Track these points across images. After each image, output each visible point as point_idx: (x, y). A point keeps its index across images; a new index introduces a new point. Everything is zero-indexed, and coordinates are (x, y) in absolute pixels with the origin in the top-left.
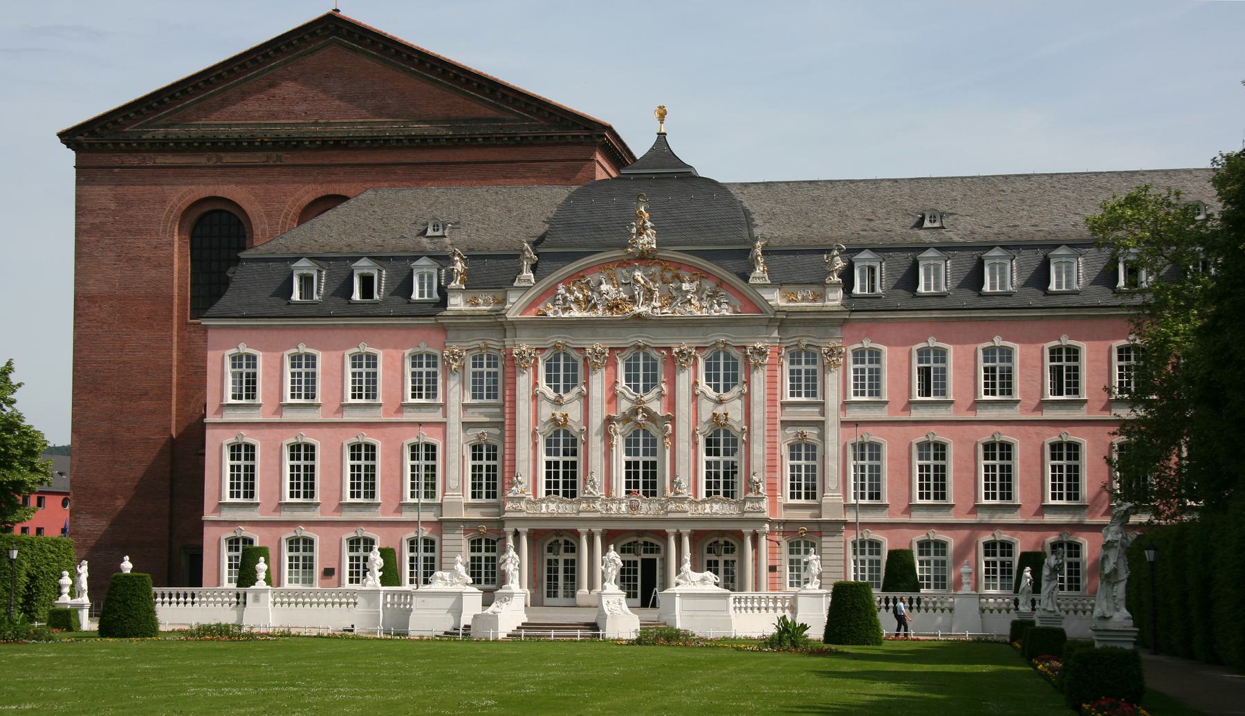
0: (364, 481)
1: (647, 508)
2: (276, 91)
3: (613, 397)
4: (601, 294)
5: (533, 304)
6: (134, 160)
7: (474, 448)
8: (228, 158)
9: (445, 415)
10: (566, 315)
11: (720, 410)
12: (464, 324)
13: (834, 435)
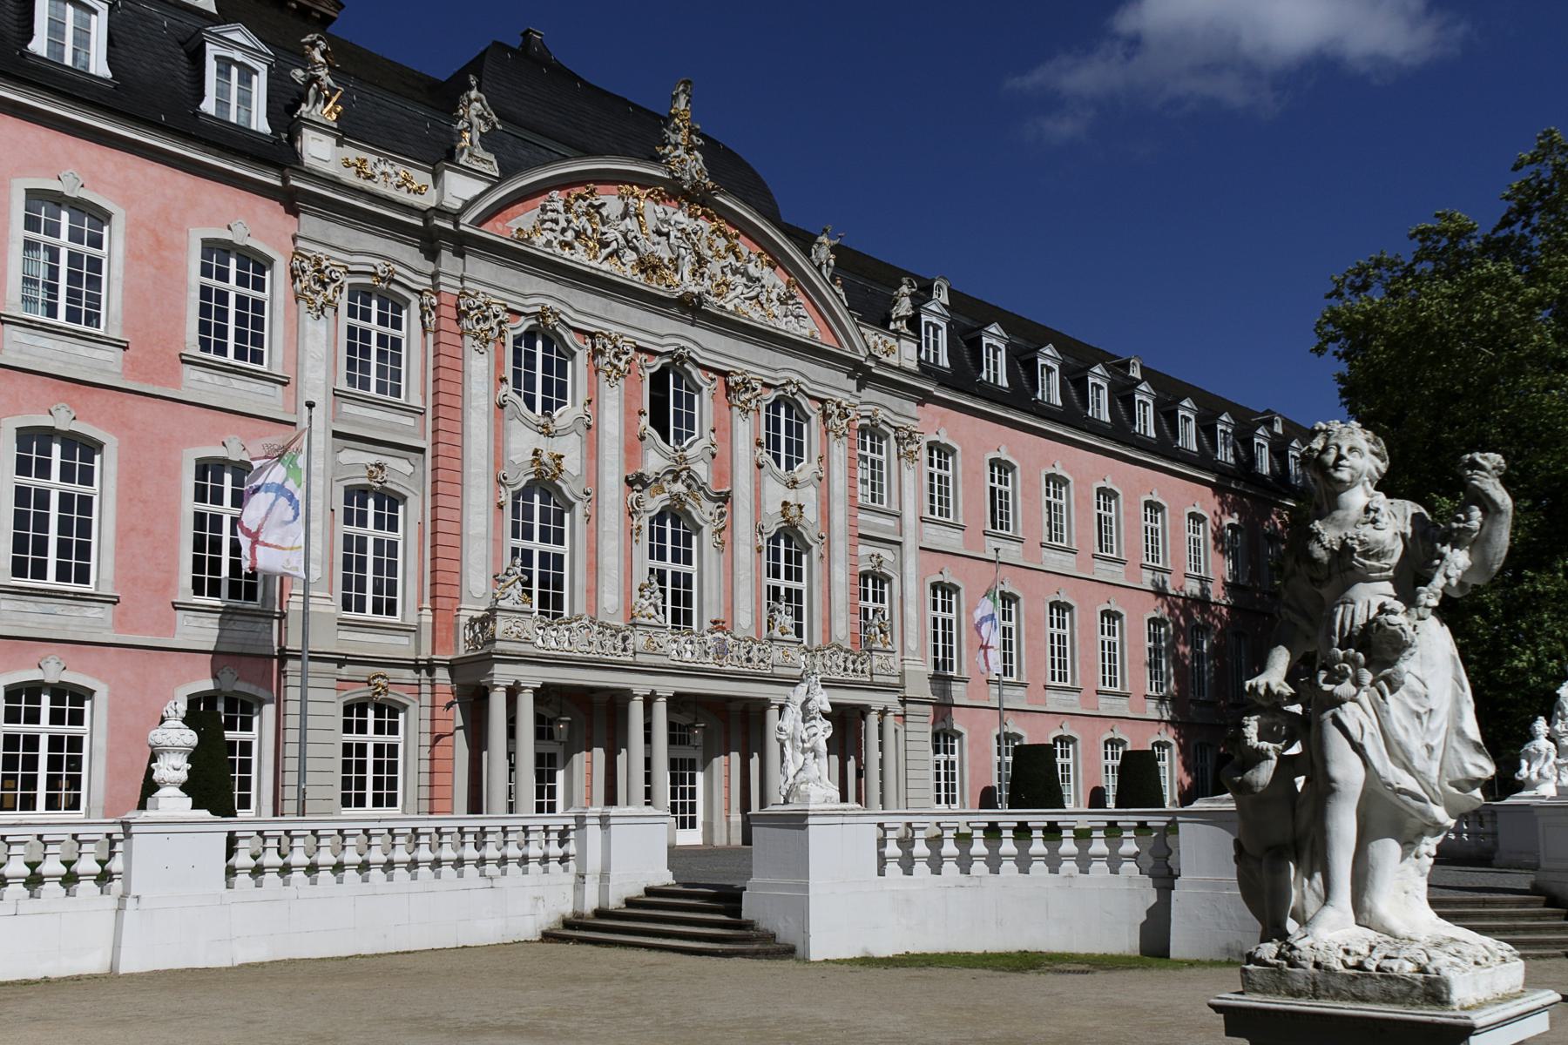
11: (791, 497)
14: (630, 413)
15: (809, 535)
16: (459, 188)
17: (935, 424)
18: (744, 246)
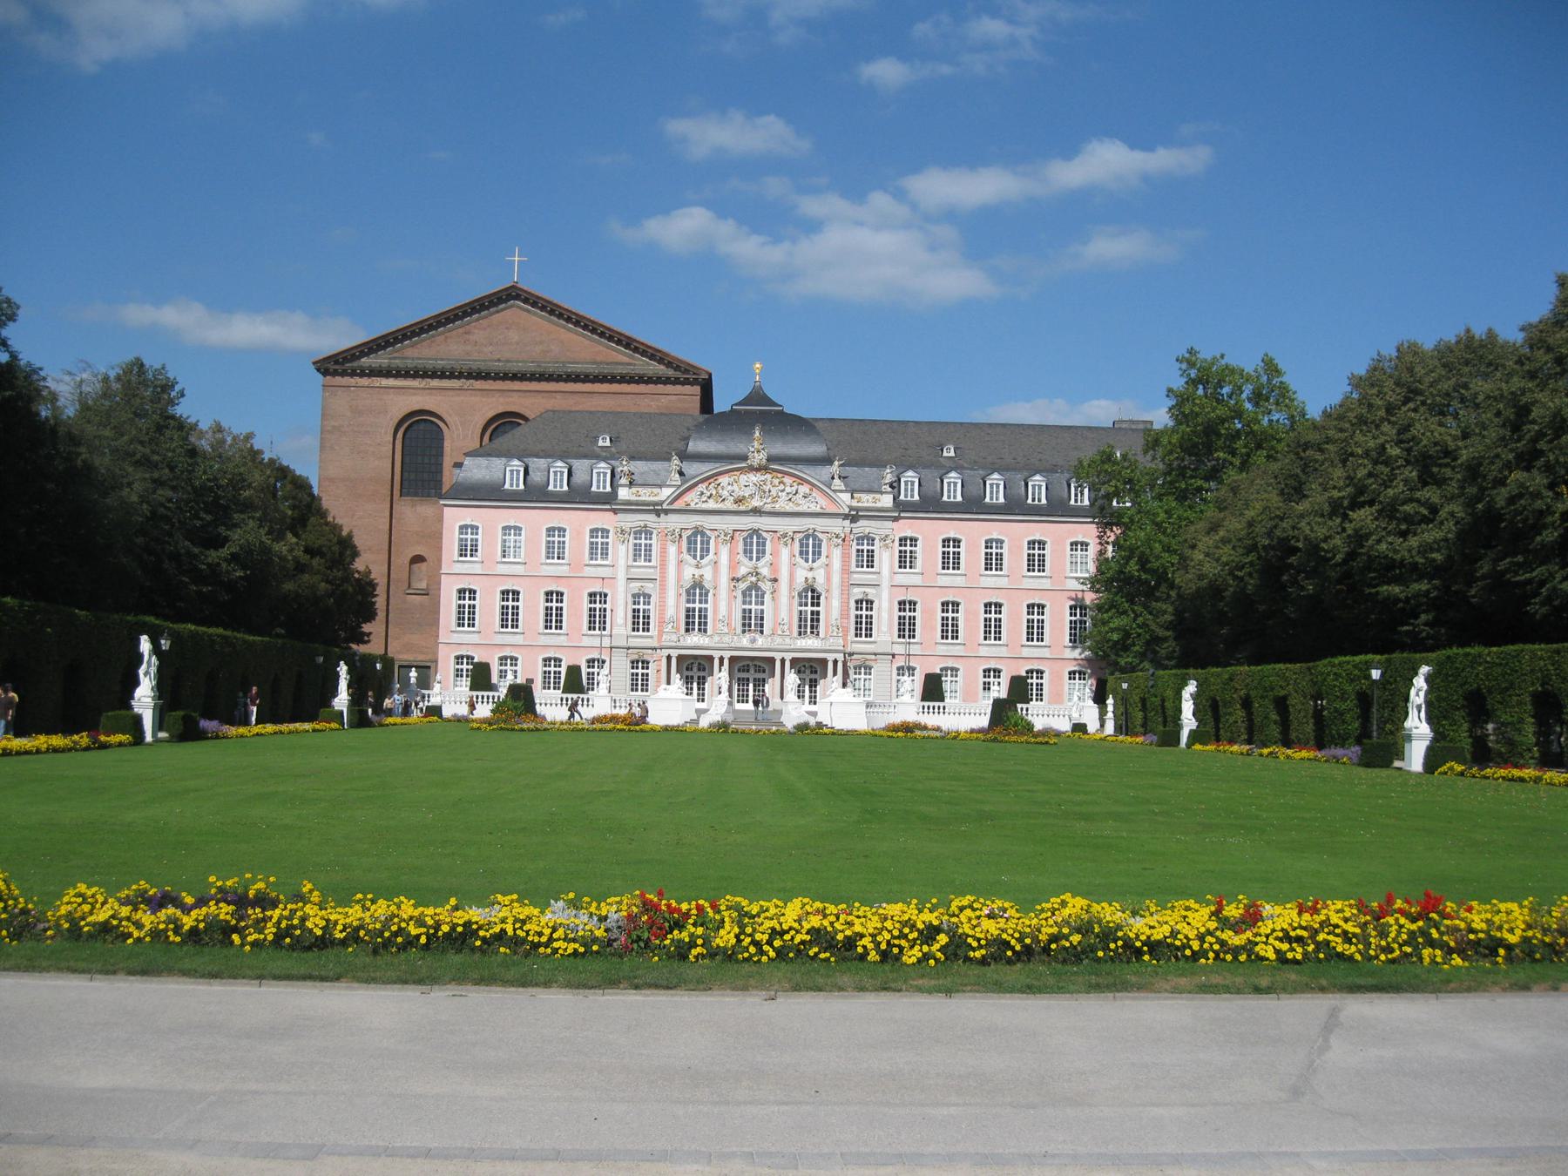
0: (553, 619)
1: (761, 642)
2: (472, 337)
3: (733, 565)
6: (365, 381)
8: (435, 383)
11: (810, 575)
13: (885, 595)
14: (732, 553)
15: (819, 589)
16: (666, 492)
17: (906, 528)
18: (788, 480)
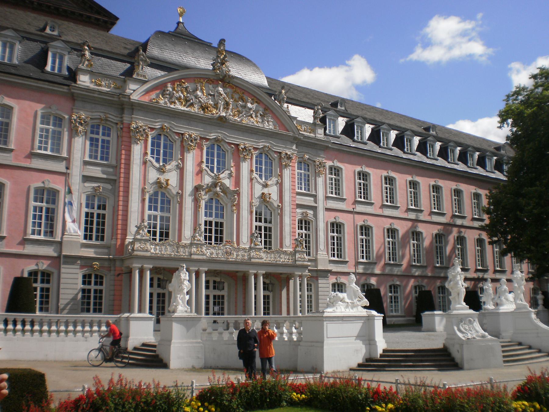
4: (197, 97)
5: (147, 92)
7: (88, 198)
9: (67, 168)
10: (172, 106)
11: (266, 191)
12: (88, 98)
